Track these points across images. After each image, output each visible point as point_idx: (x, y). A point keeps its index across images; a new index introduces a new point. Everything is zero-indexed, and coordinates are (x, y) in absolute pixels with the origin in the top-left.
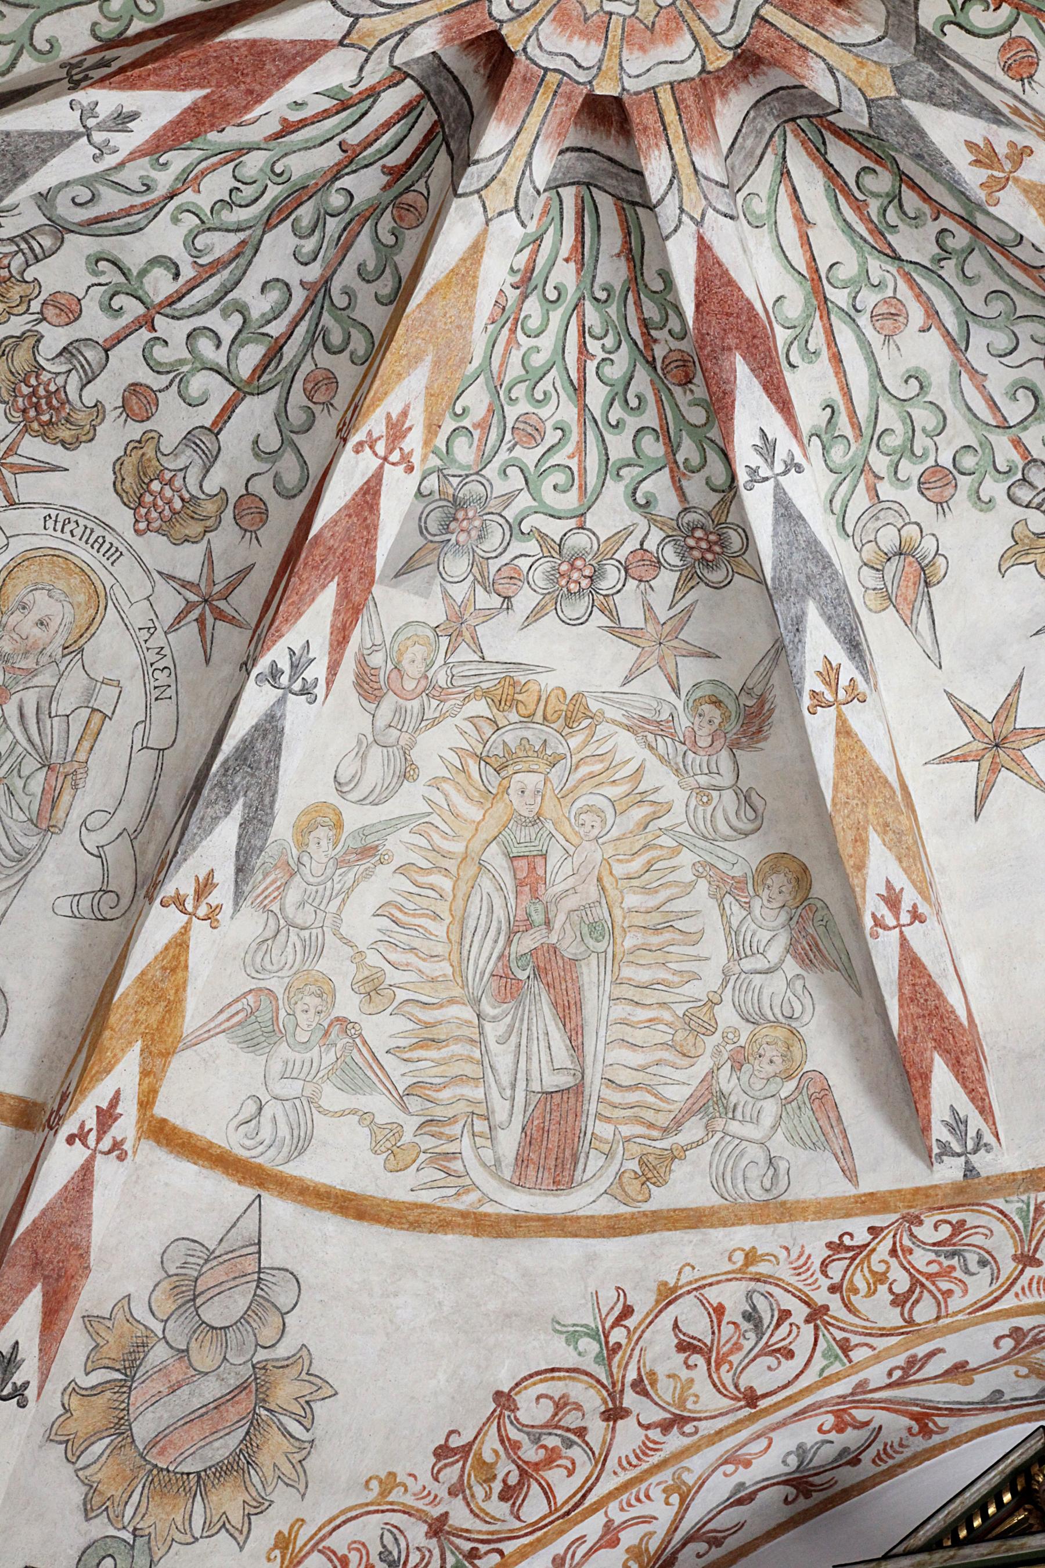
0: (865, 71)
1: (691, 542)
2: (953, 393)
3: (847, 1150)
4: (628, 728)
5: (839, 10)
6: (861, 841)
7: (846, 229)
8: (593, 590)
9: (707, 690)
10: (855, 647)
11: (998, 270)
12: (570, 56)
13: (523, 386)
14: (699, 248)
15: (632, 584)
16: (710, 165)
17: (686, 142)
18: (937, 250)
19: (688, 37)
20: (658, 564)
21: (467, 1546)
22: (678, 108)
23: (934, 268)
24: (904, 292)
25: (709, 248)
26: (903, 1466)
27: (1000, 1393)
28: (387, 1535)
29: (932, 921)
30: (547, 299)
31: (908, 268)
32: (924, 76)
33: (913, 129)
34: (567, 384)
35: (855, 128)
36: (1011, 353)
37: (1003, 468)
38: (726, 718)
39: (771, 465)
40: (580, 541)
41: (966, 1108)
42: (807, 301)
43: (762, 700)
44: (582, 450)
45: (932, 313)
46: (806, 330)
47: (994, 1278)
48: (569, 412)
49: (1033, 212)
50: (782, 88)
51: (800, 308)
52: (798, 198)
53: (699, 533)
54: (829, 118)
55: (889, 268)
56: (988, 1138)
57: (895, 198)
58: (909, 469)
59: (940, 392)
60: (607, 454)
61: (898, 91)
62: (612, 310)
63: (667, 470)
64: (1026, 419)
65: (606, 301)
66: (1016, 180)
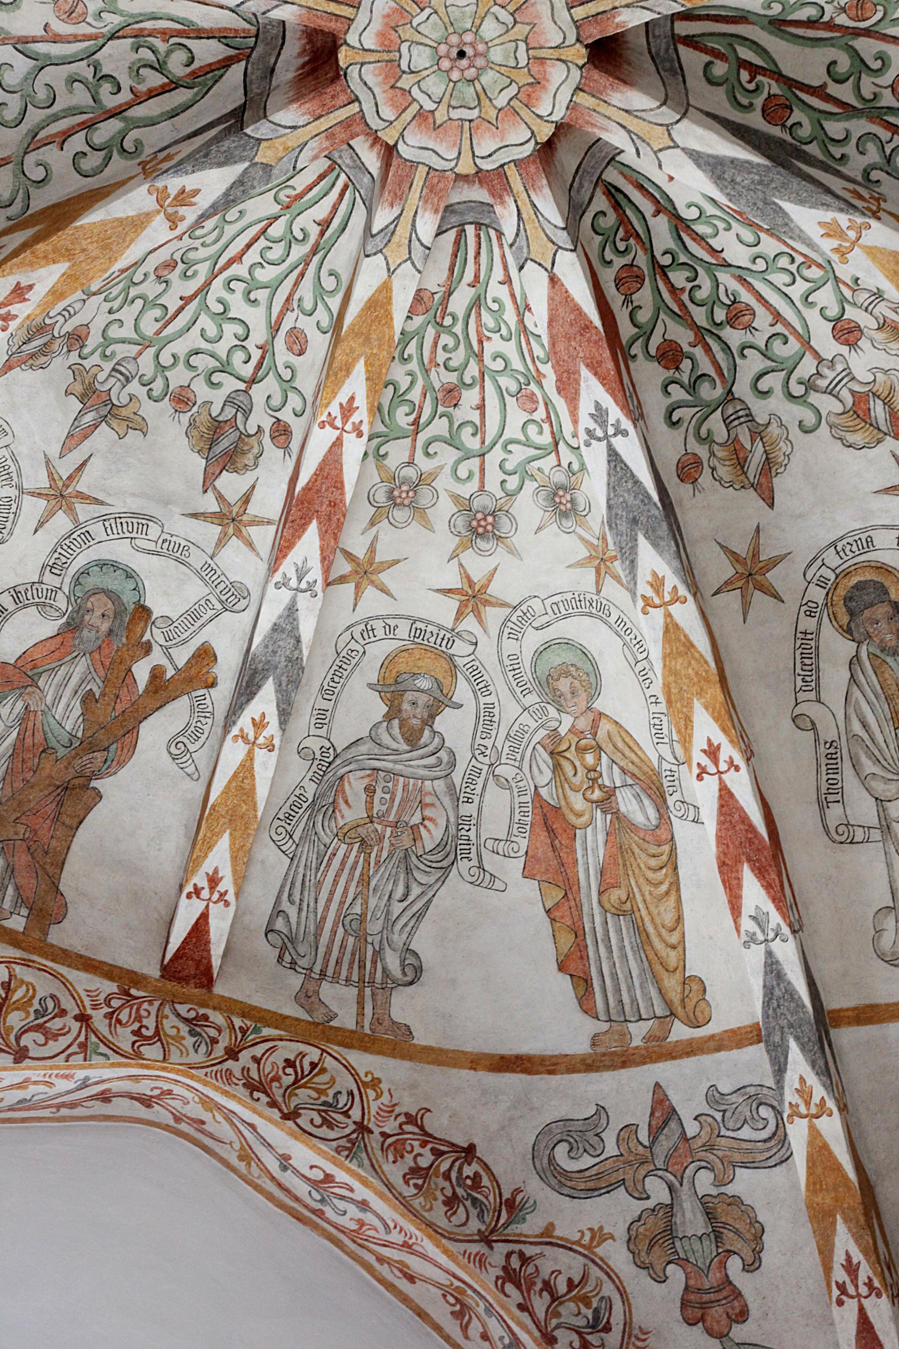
0: (281, 148)
17: (309, 8)
19: (373, 47)
22: (334, 15)
31: (101, 41)
35: (227, 75)
45: (56, 39)
49: (131, 213)
50: (283, 44)
54: (243, 63)
55: (107, 28)
61: (256, 164)
66: (158, 212)
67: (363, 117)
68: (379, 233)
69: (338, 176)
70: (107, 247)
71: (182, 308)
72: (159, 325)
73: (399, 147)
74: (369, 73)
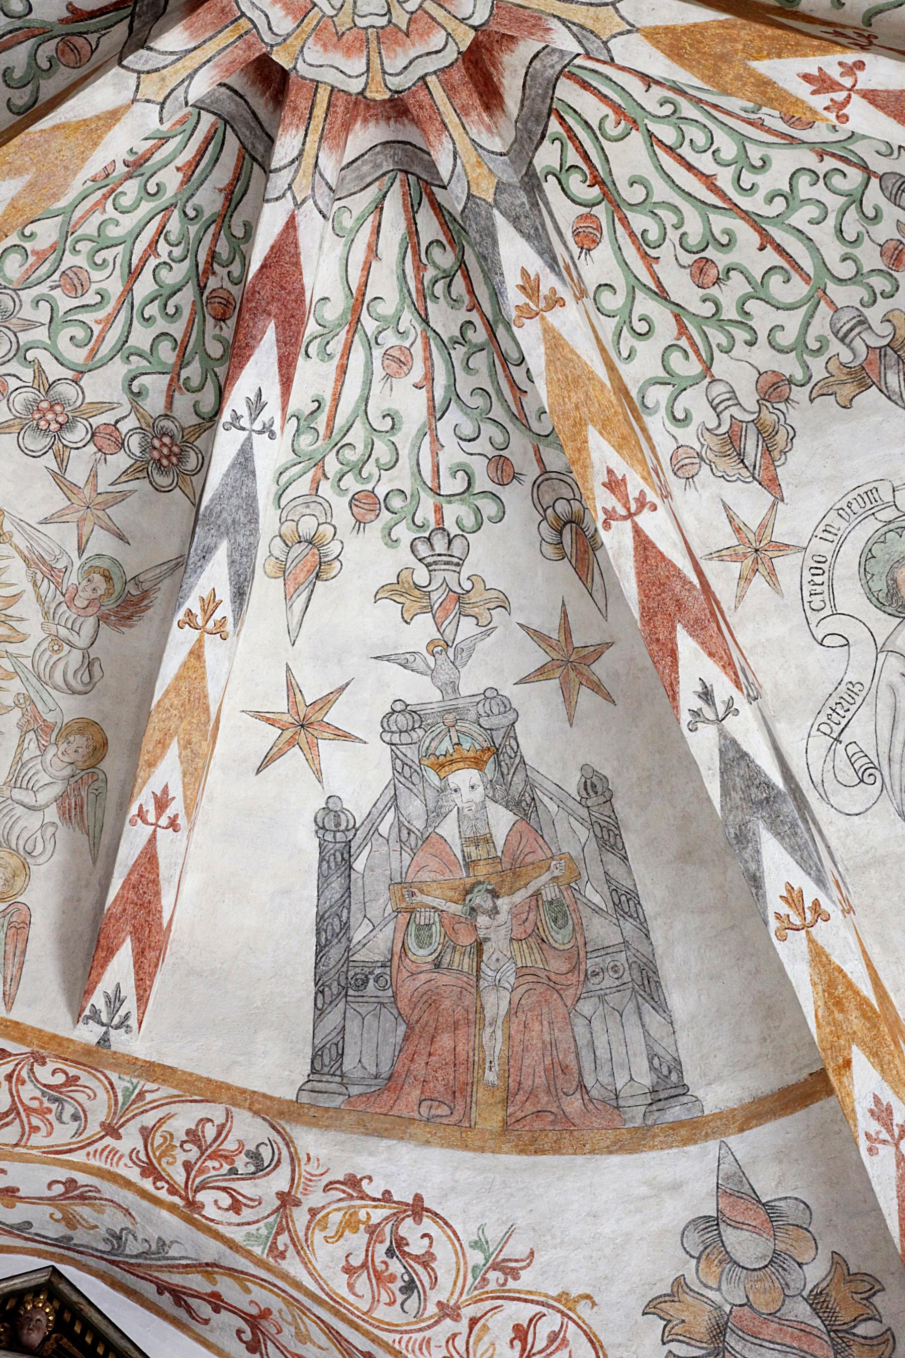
0: (479, 171)
1: (156, 443)
2: (413, 446)
3: (16, 980)
4: (25, 559)
5: (484, 115)
6: (163, 745)
7: (401, 277)
8: (57, 436)
9: (105, 564)
10: (240, 594)
11: (493, 375)
12: (267, 16)
13: (90, 245)
14: (287, 223)
15: (91, 448)
16: (329, 167)
17: (321, 138)
18: (458, 334)
19: (364, 61)
20: (121, 445)
22: (328, 109)
23: (449, 346)
24: (418, 349)
25: (295, 228)
27: (30, 1224)
29: (182, 834)
30: (146, 189)
31: (430, 334)
32: (518, 202)
33: (490, 234)
34: (126, 265)
36: (469, 441)
37: (419, 520)
38: (108, 593)
39: (253, 421)
40: (68, 391)
41: (129, 991)
42: (344, 313)
43: (145, 594)
44: (109, 322)
45: (430, 378)
46: (332, 334)
47: (78, 1133)
48: (115, 287)
49: (542, 349)
50: (410, 144)
51: (337, 315)
52: (378, 232)
53: (166, 440)
54: (433, 188)
56: (133, 1022)
57: (449, 277)
58: (351, 483)
59: (404, 439)
60: (127, 337)
61: (495, 200)
62: (193, 229)
63: (168, 377)
64: (454, 495)
65: (192, 219)
66: (543, 318)
67: (442, 70)
68: (583, 46)
69: (579, 67)
70: (576, 381)
71: (780, 250)
72: (796, 277)
73: (477, 24)
74: (394, 64)
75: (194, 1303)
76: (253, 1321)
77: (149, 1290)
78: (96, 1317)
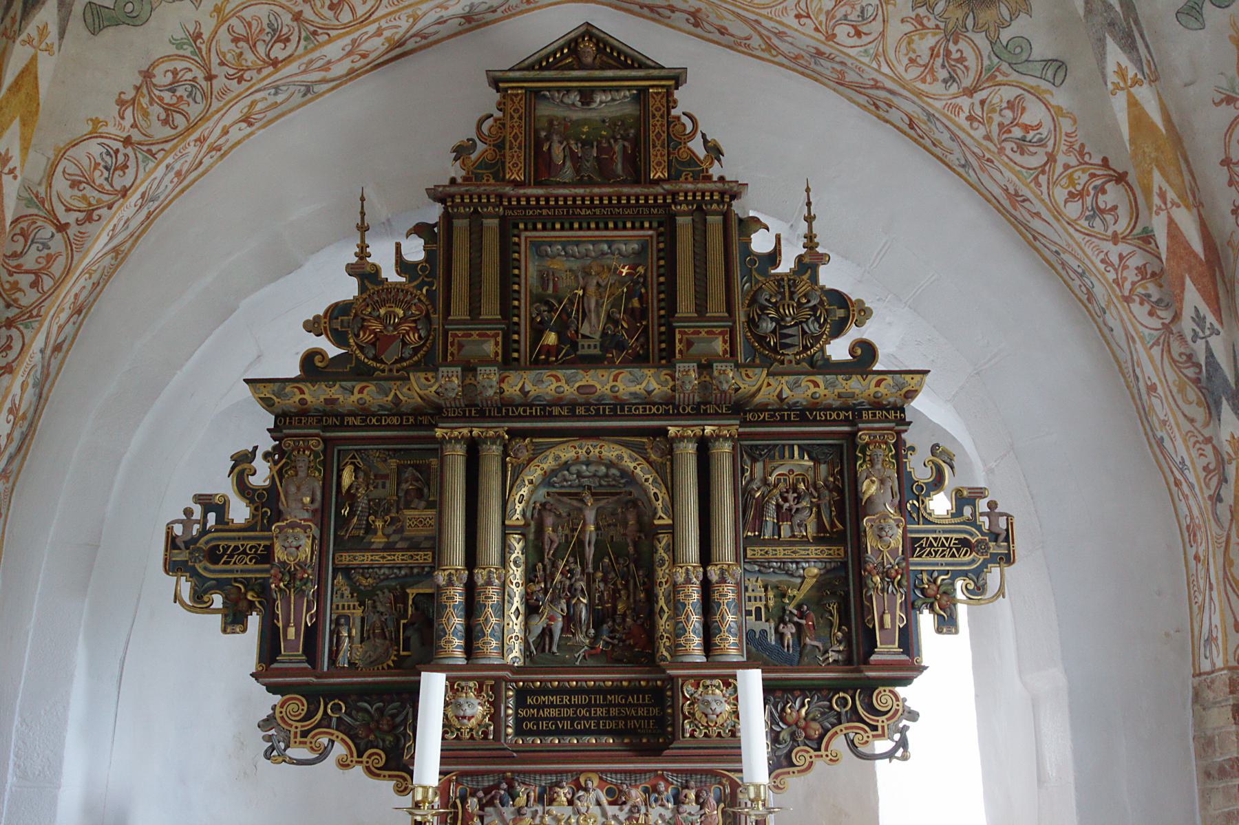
21: (312, 29)
26: (514, 15)
28: (271, 16)
75: (661, 10)
76: (693, 14)
77: (637, 8)
78: (616, 43)
